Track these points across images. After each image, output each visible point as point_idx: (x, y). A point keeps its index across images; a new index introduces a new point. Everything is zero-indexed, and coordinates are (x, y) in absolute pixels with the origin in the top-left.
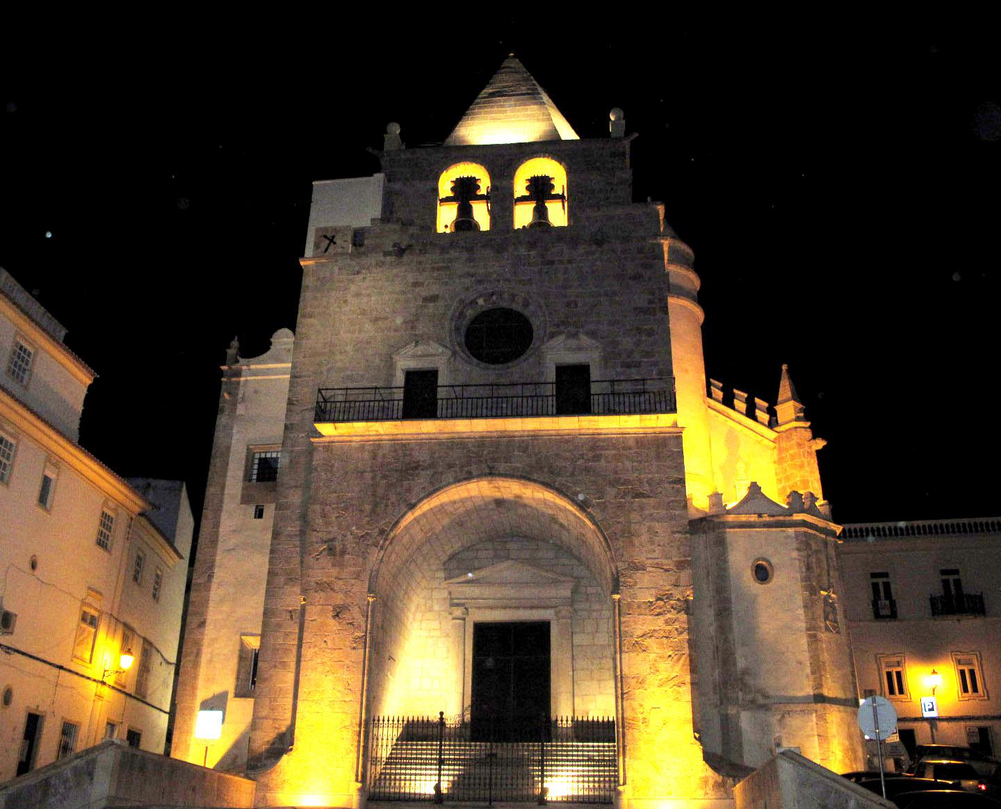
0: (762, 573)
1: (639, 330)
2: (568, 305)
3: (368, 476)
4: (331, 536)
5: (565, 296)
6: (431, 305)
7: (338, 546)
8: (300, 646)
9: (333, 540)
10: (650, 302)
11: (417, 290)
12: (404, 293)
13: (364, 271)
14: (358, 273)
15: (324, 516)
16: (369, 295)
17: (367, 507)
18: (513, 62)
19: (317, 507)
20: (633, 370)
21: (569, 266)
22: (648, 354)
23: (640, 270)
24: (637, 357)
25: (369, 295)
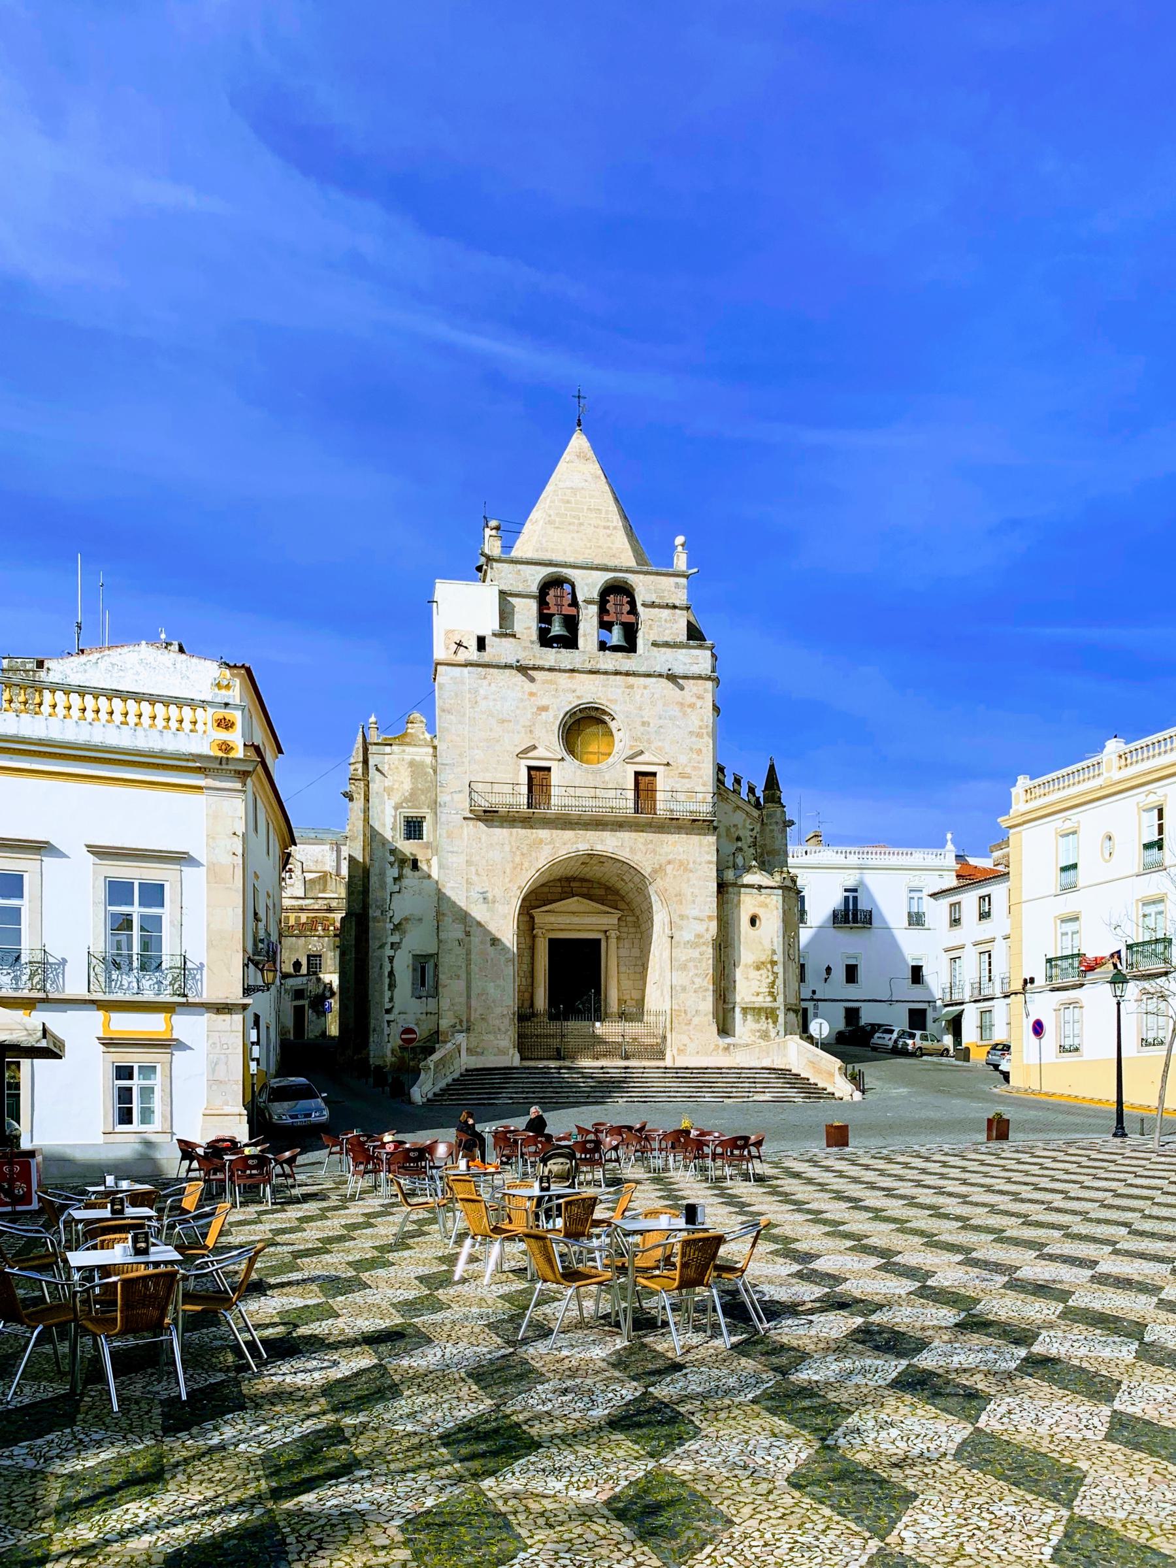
0: (753, 921)
1: (691, 749)
2: (643, 724)
3: (507, 848)
4: (485, 890)
5: (642, 717)
6: (543, 713)
7: (490, 896)
8: (468, 965)
9: (487, 892)
10: (700, 727)
11: (533, 699)
12: (522, 700)
13: (489, 677)
14: (485, 678)
15: (477, 874)
16: (494, 700)
17: (508, 871)
18: (579, 442)
19: (473, 869)
20: (686, 780)
21: (645, 692)
22: (694, 768)
23: (694, 700)
24: (688, 770)
25: (494, 700)
